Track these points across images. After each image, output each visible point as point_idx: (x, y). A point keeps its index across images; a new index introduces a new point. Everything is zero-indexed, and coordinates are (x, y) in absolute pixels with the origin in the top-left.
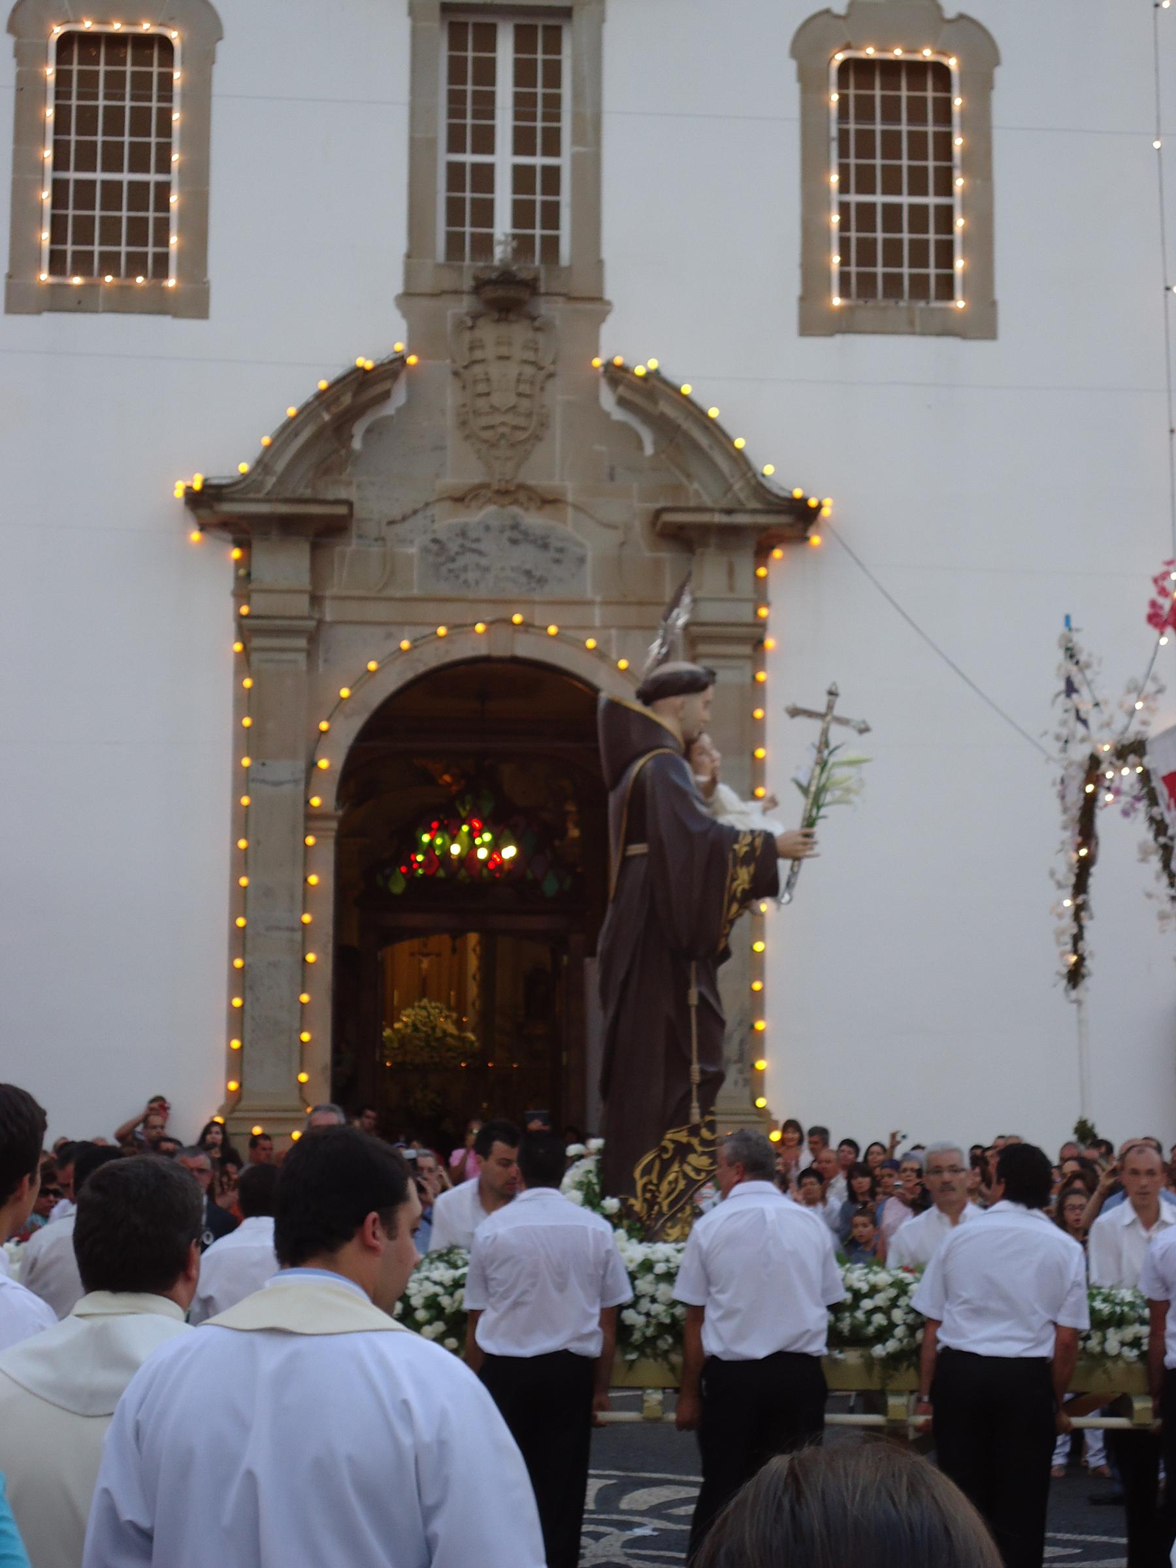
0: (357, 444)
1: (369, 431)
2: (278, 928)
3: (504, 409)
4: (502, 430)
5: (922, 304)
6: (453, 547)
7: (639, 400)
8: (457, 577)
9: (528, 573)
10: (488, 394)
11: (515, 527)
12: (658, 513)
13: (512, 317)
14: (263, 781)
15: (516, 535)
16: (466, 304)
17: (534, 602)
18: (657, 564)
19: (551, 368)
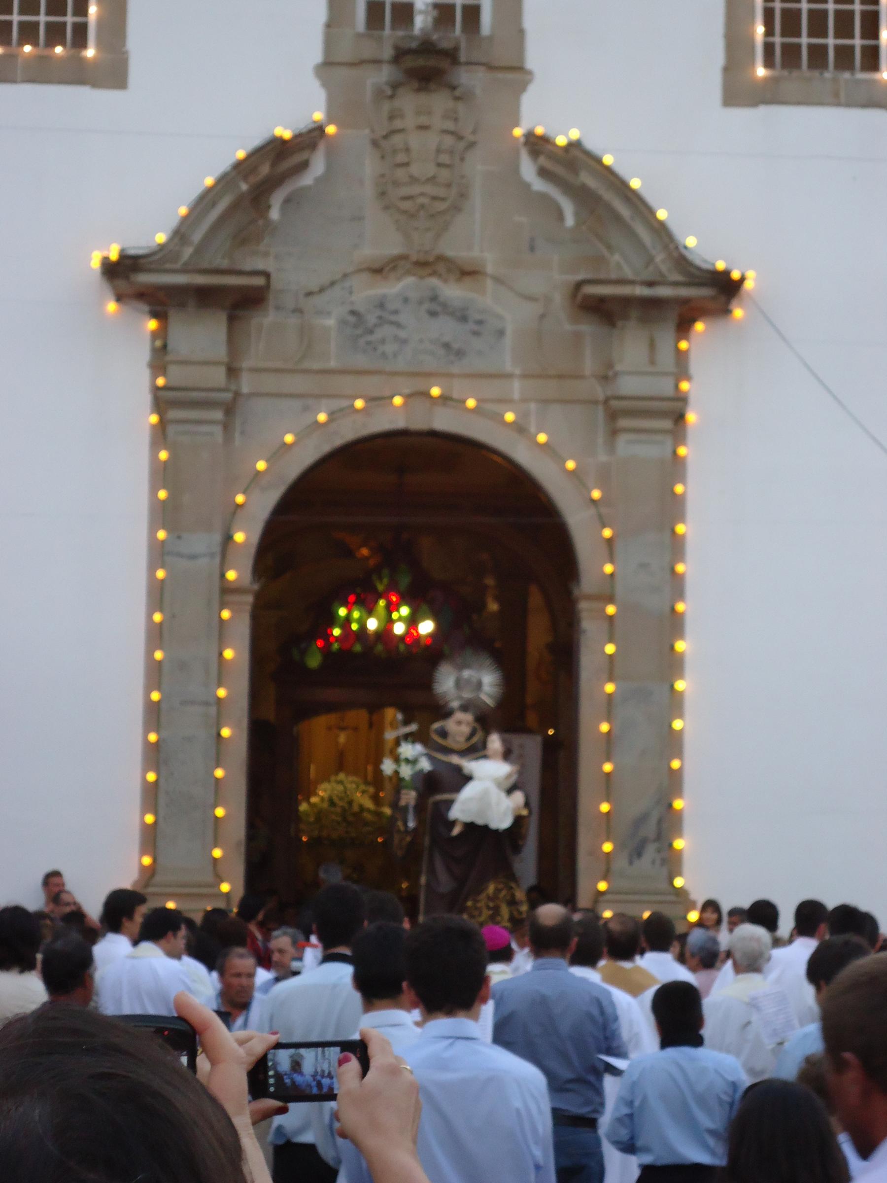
0: (275, 214)
1: (287, 201)
2: (193, 703)
5: (847, 75)
6: (371, 319)
7: (560, 170)
8: (375, 349)
9: (447, 346)
10: (406, 164)
11: (434, 298)
12: (579, 285)
14: (180, 555)
15: (435, 307)
16: (385, 74)
18: (578, 337)
19: (471, 138)
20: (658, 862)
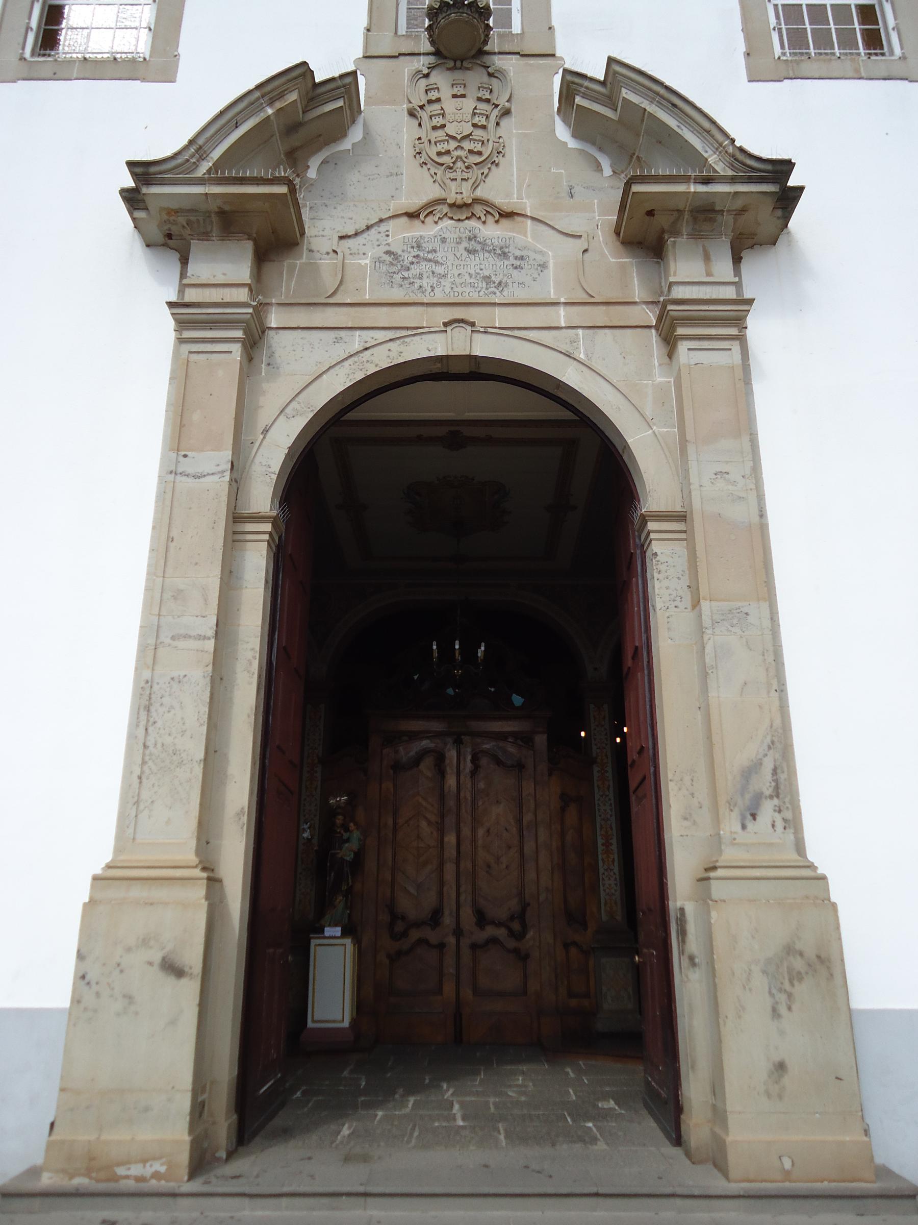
0: (312, 174)
2: (187, 637)
3: (459, 137)
4: (456, 154)
6: (408, 258)
9: (487, 279)
10: (444, 126)
11: (472, 238)
13: (465, 64)
14: (187, 475)
15: (473, 245)
17: (494, 304)
18: (622, 266)
20: (780, 824)
